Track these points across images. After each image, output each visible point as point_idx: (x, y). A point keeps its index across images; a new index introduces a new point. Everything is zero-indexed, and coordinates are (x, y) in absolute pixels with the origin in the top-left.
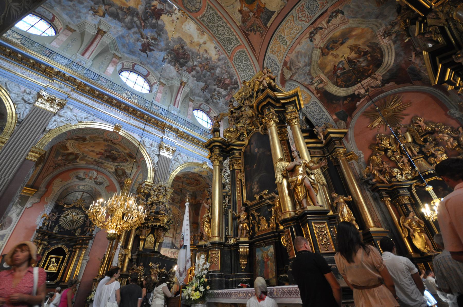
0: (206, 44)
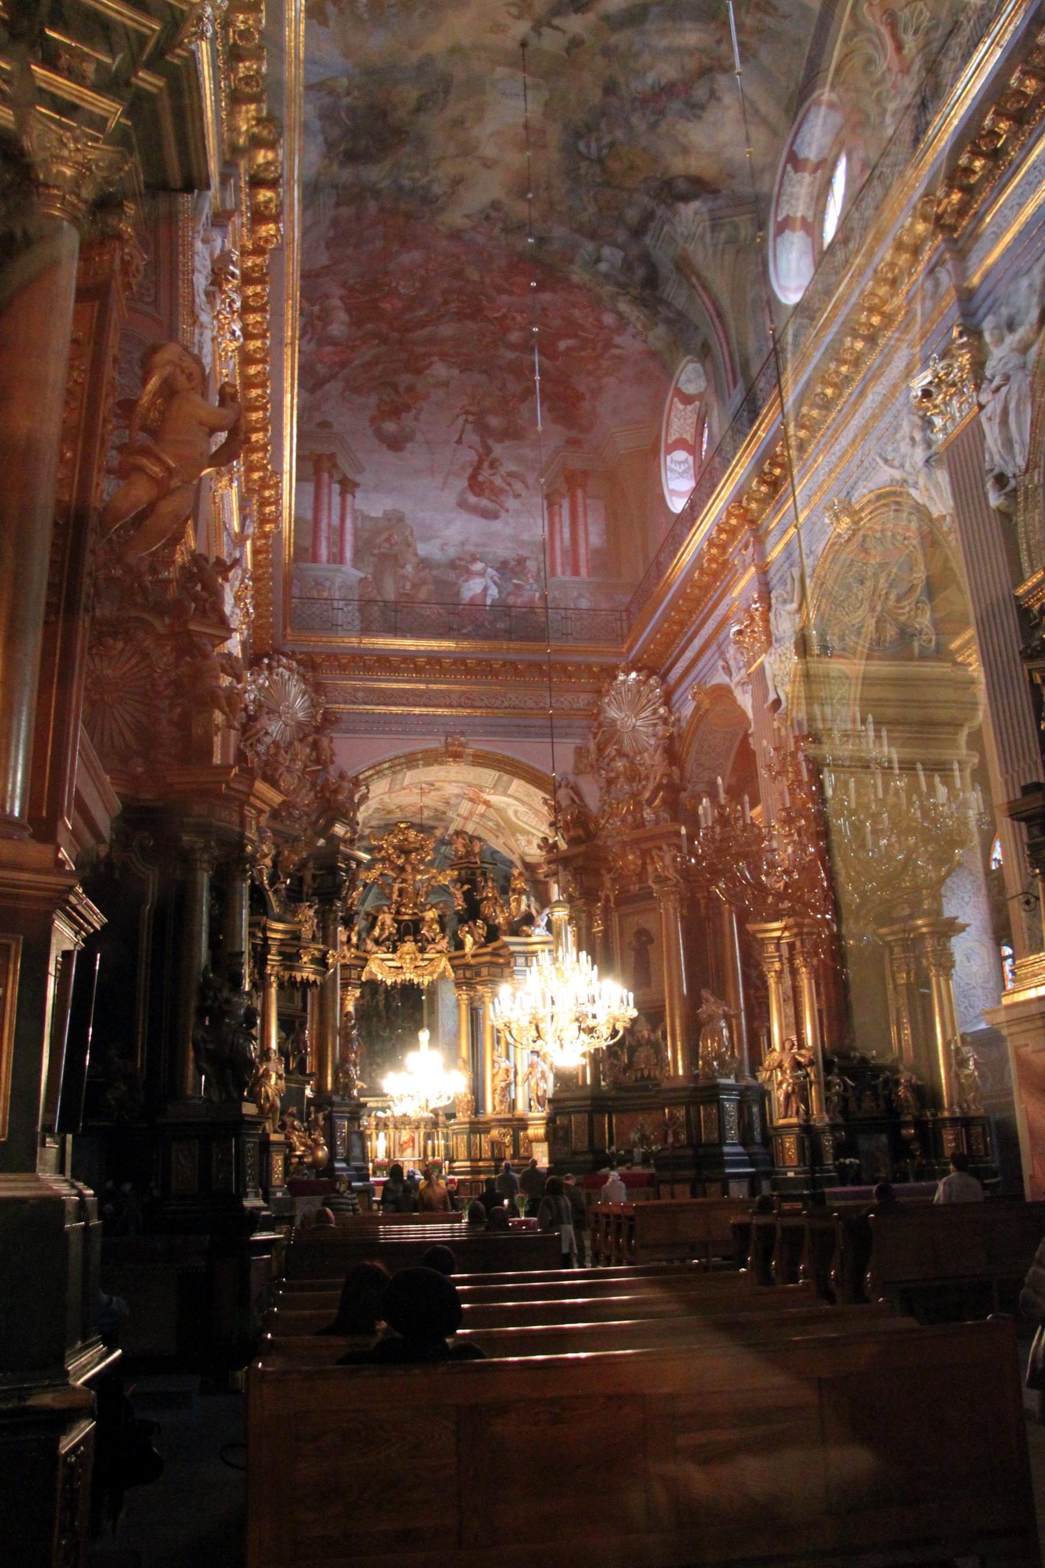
0: (488, 167)
